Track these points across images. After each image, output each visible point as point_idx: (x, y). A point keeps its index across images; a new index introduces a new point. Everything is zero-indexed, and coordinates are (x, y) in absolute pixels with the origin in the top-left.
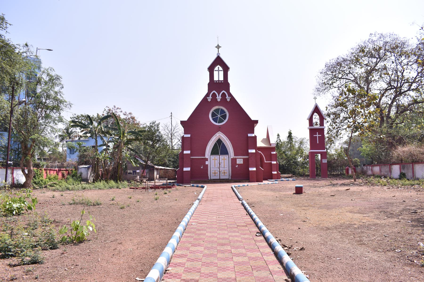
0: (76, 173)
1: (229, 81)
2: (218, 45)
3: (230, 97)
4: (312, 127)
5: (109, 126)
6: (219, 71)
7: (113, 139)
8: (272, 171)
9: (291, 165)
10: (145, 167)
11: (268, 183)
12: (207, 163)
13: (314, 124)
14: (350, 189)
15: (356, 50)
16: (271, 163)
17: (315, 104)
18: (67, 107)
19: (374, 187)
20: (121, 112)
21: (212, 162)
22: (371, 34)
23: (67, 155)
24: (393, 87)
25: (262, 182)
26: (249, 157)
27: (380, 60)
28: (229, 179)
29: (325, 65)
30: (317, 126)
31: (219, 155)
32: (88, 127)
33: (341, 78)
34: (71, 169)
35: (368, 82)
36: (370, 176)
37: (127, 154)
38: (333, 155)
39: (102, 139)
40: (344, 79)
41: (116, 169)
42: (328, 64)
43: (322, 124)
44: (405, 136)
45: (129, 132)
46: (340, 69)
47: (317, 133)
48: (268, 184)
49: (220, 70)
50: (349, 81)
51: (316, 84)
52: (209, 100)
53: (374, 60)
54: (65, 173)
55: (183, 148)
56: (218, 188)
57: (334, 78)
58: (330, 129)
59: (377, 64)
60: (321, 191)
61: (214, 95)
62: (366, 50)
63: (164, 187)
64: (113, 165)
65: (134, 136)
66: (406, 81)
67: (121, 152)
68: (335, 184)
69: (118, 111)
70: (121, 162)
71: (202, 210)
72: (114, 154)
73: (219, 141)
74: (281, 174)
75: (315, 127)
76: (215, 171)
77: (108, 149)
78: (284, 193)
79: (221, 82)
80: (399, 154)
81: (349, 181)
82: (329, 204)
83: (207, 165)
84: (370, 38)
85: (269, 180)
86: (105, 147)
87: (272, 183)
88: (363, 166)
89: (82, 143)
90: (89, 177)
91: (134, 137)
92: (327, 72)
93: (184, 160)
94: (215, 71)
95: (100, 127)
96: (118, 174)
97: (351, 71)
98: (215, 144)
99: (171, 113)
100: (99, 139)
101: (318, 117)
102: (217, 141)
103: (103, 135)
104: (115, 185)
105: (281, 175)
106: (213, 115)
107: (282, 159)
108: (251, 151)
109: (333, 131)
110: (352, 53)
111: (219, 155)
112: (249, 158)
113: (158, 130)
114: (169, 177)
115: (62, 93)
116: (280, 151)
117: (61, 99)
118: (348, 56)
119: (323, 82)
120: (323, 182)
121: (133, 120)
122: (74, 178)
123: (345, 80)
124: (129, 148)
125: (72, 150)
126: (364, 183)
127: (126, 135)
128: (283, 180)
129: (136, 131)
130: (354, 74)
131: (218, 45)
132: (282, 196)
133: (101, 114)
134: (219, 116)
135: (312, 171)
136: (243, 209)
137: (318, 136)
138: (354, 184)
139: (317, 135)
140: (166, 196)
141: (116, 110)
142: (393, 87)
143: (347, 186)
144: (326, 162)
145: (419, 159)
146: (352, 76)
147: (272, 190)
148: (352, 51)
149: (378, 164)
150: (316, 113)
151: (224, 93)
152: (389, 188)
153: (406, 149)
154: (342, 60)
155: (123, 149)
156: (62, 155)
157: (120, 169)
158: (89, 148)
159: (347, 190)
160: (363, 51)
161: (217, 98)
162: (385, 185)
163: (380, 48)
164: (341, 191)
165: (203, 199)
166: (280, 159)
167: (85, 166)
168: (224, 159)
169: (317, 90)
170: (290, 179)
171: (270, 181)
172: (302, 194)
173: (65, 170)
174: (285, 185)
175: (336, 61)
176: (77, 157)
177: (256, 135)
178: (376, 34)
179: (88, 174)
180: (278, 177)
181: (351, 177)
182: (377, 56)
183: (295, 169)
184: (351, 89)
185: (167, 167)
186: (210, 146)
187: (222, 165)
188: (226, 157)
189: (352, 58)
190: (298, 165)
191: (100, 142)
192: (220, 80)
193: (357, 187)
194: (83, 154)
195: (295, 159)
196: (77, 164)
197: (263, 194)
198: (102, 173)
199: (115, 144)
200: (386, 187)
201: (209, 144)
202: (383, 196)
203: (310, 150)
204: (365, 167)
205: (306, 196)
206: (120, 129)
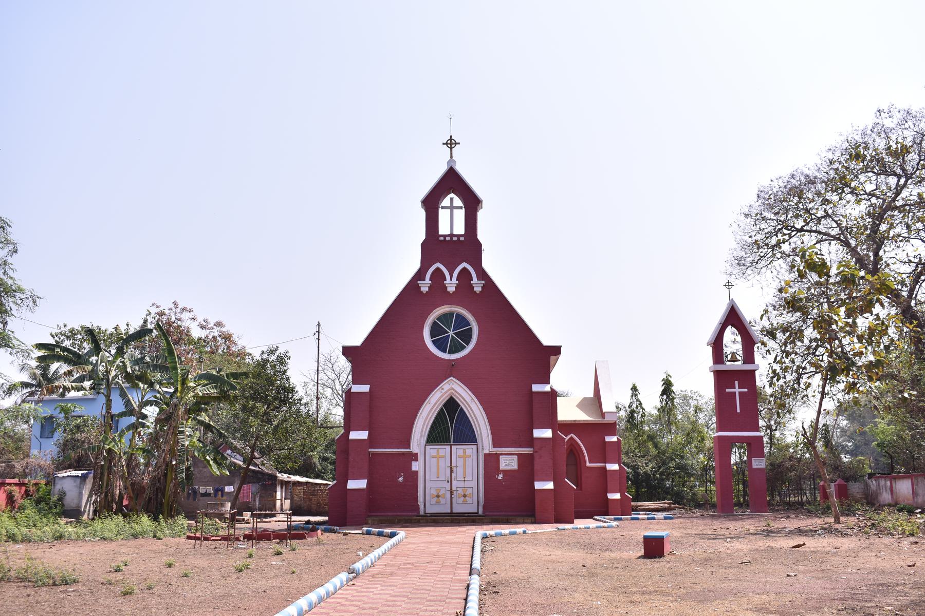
0: (49, 494)
1: (479, 237)
2: (451, 139)
3: (483, 282)
4: (720, 367)
5: (147, 359)
6: (452, 208)
7: (155, 397)
8: (606, 492)
9: (669, 474)
10: (247, 476)
11: (587, 525)
12: (415, 466)
14: (804, 544)
15: (842, 155)
17: (728, 301)
18: (26, 304)
19: (877, 540)
20: (194, 319)
21: (431, 462)
22: (879, 111)
23: (33, 438)
25: (572, 522)
26: (535, 452)
27: (906, 181)
28: (478, 513)
29: (757, 192)
30: (736, 363)
31: (451, 445)
32: (88, 360)
33: (801, 230)
34: (33, 482)
35: (877, 241)
36: (881, 507)
37: (195, 440)
38: (788, 446)
39: (123, 395)
40: (812, 234)
41: (159, 481)
42: (766, 190)
43: (749, 357)
45: (201, 377)
46: (801, 206)
47: (737, 382)
48: (585, 528)
49: (455, 205)
50: (824, 237)
51: (734, 245)
52: (425, 289)
53: (892, 181)
54: (17, 492)
55: (349, 423)
56: (436, 539)
57: (781, 229)
58: (774, 371)
59: (898, 194)
60: (722, 550)
61: (438, 274)
62: (869, 154)
63: (292, 534)
64: (154, 471)
65: (216, 387)
67: (176, 432)
68: (776, 530)
69: (185, 316)
70: (174, 463)
71: (343, 600)
72: (157, 439)
73: (451, 405)
74: (634, 500)
75: (729, 365)
76: (439, 489)
77: (143, 426)
78: (613, 555)
79: (459, 239)
82: (718, 585)
83: (417, 472)
84: (877, 121)
85: (596, 517)
86: (133, 419)
87: (597, 527)
89: (73, 408)
90: (84, 504)
91: (213, 391)
92: (763, 212)
93: (351, 459)
94: (443, 208)
95: (121, 362)
96: (167, 497)
97: (830, 212)
98: (439, 414)
99: (319, 324)
100: (116, 397)
101: (739, 338)
102: (445, 405)
103: (127, 385)
104: (149, 528)
105: (633, 504)
106: (436, 330)
107: (644, 456)
108: (538, 433)
109: (784, 378)
110: (831, 163)
111: (451, 445)
112: (535, 454)
113: (285, 372)
114: (321, 505)
115: (11, 266)
116: (639, 435)
117: (10, 282)
118: (822, 168)
119: (754, 239)
120: (750, 525)
121: (226, 341)
122: (43, 505)
123: (816, 235)
124: (201, 423)
125: (48, 426)
126: (859, 527)
127: (192, 384)
128: (637, 519)
129: (222, 373)
130: (839, 220)
131: (451, 139)
132: (603, 562)
133: (123, 328)
134: (451, 333)
135: (725, 492)
136: (460, 601)
138: (827, 530)
139: (737, 390)
140: (275, 561)
141: (179, 315)
143: (806, 535)
144: (763, 466)
146: (835, 225)
147: (588, 547)
148: (830, 156)
149: (907, 472)
150: (733, 325)
151: (464, 269)
152: (916, 543)
154: (803, 180)
155: (183, 424)
156: (21, 440)
157: (171, 481)
158: (90, 422)
159: (795, 547)
160: (858, 157)
161: (445, 282)
162: (912, 535)
163: (905, 150)
164: (779, 550)
165: (372, 569)
166: (639, 457)
167: (74, 473)
168: (465, 457)
169: (736, 261)
170: (660, 515)
171: (598, 520)
172: (661, 559)
173: (16, 484)
174: (631, 533)
175: (785, 184)
176: (56, 447)
177: (556, 388)
178: (892, 110)
179: (81, 494)
180: (623, 509)
181: (826, 511)
182: (899, 171)
183: (683, 486)
184: (814, 263)
185: (317, 476)
186: (426, 418)
187: (459, 473)
188: (470, 449)
189: (832, 173)
190: (690, 475)
191: (118, 406)
192: (455, 233)
193: (831, 540)
194: (72, 439)
195: (682, 457)
196: (52, 467)
197: (553, 557)
198: (120, 493)
199: (161, 410)
200: (912, 539)
201: (423, 413)
202: (882, 564)
203: (717, 432)
204: (874, 482)
205: (669, 565)
206: (176, 368)
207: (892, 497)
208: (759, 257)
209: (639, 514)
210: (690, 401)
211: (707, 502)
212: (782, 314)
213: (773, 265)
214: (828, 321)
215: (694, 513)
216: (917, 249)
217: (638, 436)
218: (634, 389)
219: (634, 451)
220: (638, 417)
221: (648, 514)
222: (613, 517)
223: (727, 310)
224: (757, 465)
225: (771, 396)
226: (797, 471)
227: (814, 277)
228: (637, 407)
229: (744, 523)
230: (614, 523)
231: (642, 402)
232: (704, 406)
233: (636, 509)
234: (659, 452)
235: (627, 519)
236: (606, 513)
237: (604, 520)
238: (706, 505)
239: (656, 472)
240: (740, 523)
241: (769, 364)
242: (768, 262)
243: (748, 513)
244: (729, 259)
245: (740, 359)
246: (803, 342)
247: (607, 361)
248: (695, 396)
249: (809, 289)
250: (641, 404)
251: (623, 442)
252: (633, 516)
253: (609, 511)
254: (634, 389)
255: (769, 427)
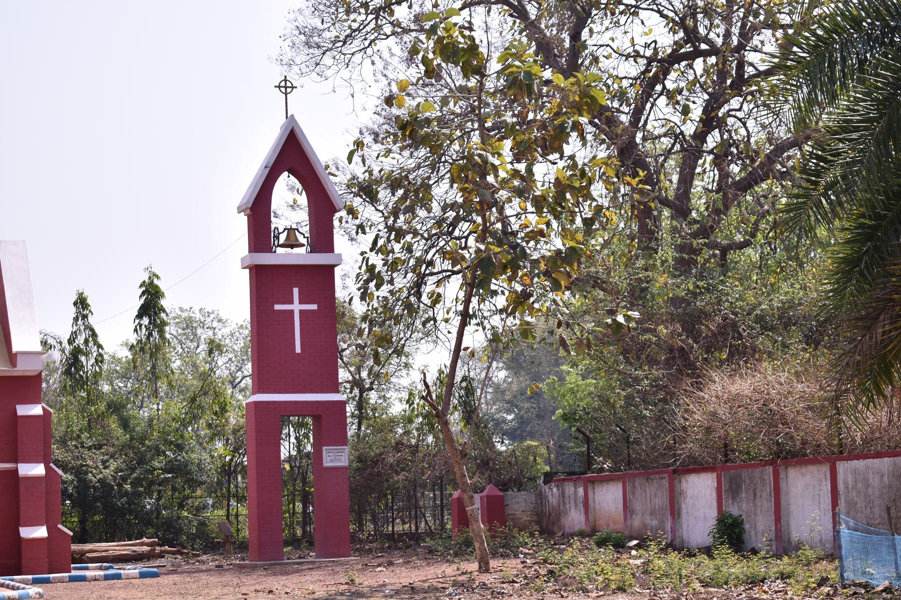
4: (265, 259)
9: (151, 483)
13: (278, 238)
16: (16, 470)
17: (283, 120)
24: (704, 46)
30: (296, 250)
38: (393, 422)
44: (749, 314)
47: (296, 291)
58: (371, 269)
66: (762, 18)
68: (366, 590)
75: (282, 255)
80: (714, 414)
81: (450, 570)
88: (545, 483)
101: (303, 200)
105: (74, 547)
109: (391, 282)
116: (89, 402)
126: (526, 577)
128: (83, 579)
137: (301, 312)
139: (296, 307)
142: (704, 46)
145: (804, 443)
150: (292, 172)
153: (743, 386)
166: (89, 448)
169: (303, 37)
170: (131, 570)
181: (464, 549)
183: (181, 506)
184: (454, 44)
190: (194, 484)
195: (180, 448)
203: (254, 393)
204: (555, 490)
207: (587, 519)
208: (349, 31)
209: (87, 569)
210: (199, 331)
211: (228, 538)
212: (389, 151)
213: (376, 48)
214: (480, 166)
215: (203, 562)
216: (651, 31)
217: (88, 403)
218: (81, 303)
219: (79, 436)
220: (87, 363)
221: (107, 568)
222: (30, 577)
223: (280, 138)
224: (332, 461)
225: (364, 318)
226: (409, 471)
227: (454, 75)
228: (86, 342)
229: (303, 579)
230: (33, 590)
231: (97, 331)
232: (227, 341)
233: (80, 559)
234: (132, 439)
235: (61, 581)
236: (17, 570)
237: (13, 583)
238: (228, 545)
239: (124, 479)
240: (295, 578)
241: (362, 253)
242: (367, 43)
243: (310, 559)
244: (287, 32)
245: (304, 241)
246: (429, 210)
247: (24, 242)
248: (209, 320)
249: (445, 101)
250: (94, 335)
251: (54, 418)
252: (74, 573)
253: (24, 561)
254: (81, 303)
255: (357, 383)
